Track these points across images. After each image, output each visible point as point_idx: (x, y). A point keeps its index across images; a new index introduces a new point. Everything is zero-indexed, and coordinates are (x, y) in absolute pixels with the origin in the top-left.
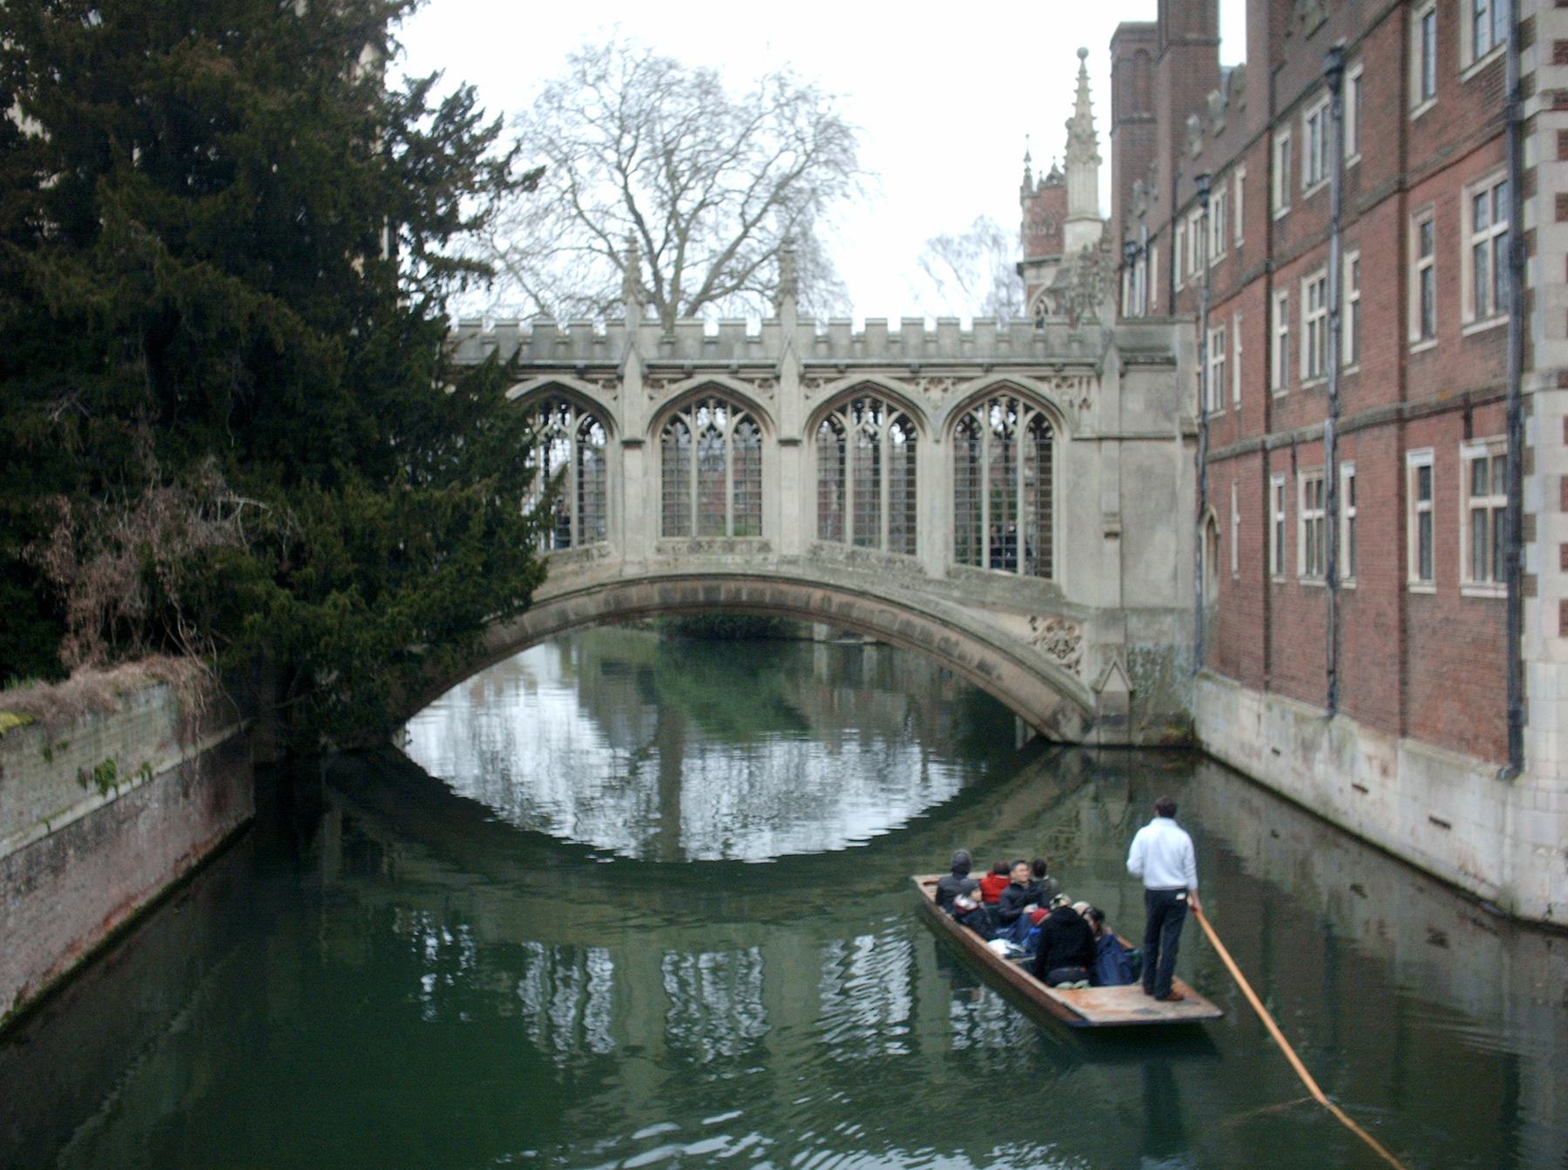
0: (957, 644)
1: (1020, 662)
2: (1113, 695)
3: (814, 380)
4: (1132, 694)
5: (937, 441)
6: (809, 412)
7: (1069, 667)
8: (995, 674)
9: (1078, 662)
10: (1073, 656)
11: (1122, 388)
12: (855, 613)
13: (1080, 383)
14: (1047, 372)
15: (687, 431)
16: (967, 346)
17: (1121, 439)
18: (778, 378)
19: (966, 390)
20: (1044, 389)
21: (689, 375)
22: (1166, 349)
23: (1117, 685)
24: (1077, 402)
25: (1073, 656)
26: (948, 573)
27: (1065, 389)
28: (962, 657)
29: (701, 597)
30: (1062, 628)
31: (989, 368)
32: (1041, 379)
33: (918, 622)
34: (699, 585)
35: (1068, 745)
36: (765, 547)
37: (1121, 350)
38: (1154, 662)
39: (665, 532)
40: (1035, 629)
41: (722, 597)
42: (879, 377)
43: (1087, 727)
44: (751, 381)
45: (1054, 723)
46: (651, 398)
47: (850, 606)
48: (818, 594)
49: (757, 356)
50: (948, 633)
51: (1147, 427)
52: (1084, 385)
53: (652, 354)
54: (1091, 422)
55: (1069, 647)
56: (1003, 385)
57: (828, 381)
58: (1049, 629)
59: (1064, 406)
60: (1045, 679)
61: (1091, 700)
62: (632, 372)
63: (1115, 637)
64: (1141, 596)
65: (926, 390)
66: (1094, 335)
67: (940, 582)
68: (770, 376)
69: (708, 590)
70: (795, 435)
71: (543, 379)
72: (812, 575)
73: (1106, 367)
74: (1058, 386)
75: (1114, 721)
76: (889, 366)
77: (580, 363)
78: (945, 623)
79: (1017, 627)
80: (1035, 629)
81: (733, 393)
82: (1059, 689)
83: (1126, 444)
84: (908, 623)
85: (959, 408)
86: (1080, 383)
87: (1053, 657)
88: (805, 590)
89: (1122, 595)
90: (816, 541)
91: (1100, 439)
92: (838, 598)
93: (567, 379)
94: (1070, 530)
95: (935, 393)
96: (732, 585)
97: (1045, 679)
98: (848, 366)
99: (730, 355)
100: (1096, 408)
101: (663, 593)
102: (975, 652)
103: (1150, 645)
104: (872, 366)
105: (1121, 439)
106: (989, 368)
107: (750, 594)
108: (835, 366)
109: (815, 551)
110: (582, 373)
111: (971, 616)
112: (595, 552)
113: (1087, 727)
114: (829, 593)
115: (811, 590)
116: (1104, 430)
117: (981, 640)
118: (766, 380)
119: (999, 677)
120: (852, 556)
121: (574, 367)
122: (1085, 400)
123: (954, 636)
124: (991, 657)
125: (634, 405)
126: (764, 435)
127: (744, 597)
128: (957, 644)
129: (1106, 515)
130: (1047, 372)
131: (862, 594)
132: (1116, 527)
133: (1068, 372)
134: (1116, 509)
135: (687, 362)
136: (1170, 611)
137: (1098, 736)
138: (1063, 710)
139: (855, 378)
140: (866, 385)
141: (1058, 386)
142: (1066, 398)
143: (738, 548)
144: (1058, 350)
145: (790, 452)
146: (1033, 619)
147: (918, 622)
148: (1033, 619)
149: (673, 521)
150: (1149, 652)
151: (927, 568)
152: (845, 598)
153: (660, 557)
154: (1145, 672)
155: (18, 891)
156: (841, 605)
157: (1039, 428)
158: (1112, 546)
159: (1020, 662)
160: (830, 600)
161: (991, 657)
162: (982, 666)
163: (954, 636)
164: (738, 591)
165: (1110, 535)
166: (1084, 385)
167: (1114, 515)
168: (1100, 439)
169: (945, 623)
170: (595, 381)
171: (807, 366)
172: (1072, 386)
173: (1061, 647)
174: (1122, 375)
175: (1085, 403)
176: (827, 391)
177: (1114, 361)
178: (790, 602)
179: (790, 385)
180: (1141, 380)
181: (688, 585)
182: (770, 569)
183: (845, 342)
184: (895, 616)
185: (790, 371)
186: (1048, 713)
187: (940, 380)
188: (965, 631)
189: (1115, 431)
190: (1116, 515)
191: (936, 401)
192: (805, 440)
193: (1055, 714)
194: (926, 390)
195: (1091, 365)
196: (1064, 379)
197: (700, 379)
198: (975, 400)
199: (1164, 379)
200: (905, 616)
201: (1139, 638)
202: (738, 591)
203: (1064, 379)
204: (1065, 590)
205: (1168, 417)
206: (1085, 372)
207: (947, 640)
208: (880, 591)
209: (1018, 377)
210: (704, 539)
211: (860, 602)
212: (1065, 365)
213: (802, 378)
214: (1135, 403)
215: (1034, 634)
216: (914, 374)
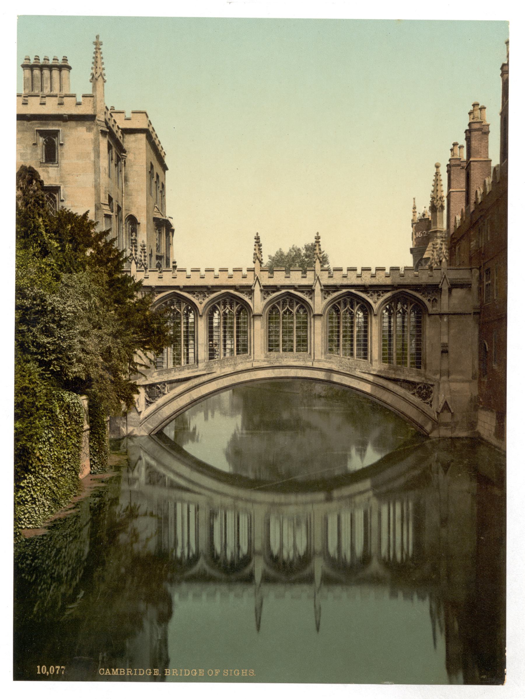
9: (431, 401)
15: (279, 311)
149: (272, 346)
170: (242, 292)
185: (318, 289)
216: (365, 288)
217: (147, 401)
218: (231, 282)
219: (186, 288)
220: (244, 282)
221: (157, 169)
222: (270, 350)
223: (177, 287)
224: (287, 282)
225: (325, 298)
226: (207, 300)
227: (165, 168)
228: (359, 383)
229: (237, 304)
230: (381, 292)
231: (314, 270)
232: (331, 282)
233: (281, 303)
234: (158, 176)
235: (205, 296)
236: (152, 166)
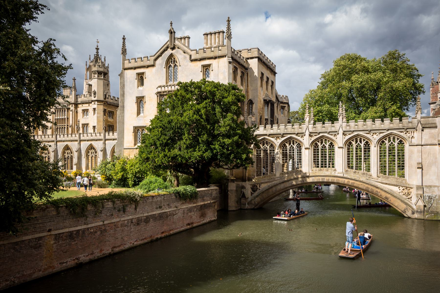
1: (395, 197)
2: (419, 206)
3: (346, 134)
4: (425, 206)
7: (409, 199)
8: (389, 200)
9: (411, 198)
10: (410, 196)
12: (355, 185)
16: (382, 125)
17: (422, 145)
19: (382, 135)
20: (402, 134)
21: (319, 134)
22: (435, 123)
23: (421, 204)
24: (411, 137)
25: (410, 196)
28: (381, 195)
29: (321, 181)
31: (388, 130)
32: (401, 132)
34: (320, 178)
35: (409, 218)
36: (335, 170)
38: (432, 198)
41: (325, 181)
42: (361, 133)
43: (413, 213)
44: (331, 135)
45: (405, 212)
47: (354, 183)
49: (333, 129)
51: (429, 143)
52: (412, 133)
53: (311, 130)
54: (414, 141)
55: (409, 194)
56: (391, 134)
57: (350, 134)
58: (403, 190)
59: (407, 138)
61: (415, 207)
62: (307, 133)
64: (428, 184)
65: (372, 135)
66: (415, 121)
68: (336, 133)
69: (322, 179)
71: (289, 136)
72: (345, 176)
74: (406, 133)
77: (296, 133)
78: (377, 188)
81: (328, 138)
82: (406, 204)
85: (380, 139)
87: (404, 196)
88: (343, 179)
92: (351, 181)
93: (294, 136)
94: (409, 167)
95: (375, 136)
96: (327, 178)
98: (354, 131)
99: (328, 130)
100: (416, 138)
101: (313, 179)
102: (384, 195)
103: (429, 195)
105: (422, 145)
106: (388, 130)
107: (331, 180)
108: (350, 131)
110: (297, 134)
113: (413, 213)
117: (385, 191)
118: (335, 135)
120: (355, 172)
124: (389, 196)
127: (330, 181)
129: (418, 163)
136: (436, 186)
138: (407, 209)
139: (355, 133)
140: (358, 135)
141: (406, 133)
142: (408, 136)
143: (329, 170)
144: (406, 125)
145: (341, 149)
146: (399, 187)
148: (399, 187)
150: (430, 196)
151: (373, 175)
154: (429, 201)
155: (135, 225)
156: (352, 183)
157: (401, 142)
159: (395, 197)
161: (389, 196)
163: (379, 190)
164: (329, 179)
165: (418, 168)
166: (412, 133)
167: (420, 163)
168: (416, 145)
170: (299, 136)
171: (344, 131)
173: (407, 194)
178: (340, 182)
179: (340, 135)
181: (318, 178)
182: (336, 174)
186: (403, 209)
187: (376, 133)
188: (382, 189)
189: (420, 143)
191: (374, 138)
192: (344, 147)
193: (405, 210)
194: (372, 135)
195: (414, 128)
197: (321, 135)
198: (384, 137)
199: (433, 131)
200: (367, 186)
201: (427, 193)
202: (329, 179)
203: (407, 132)
204: (407, 181)
205: (435, 139)
206: (412, 130)
207: (377, 191)
208: (361, 179)
210: (322, 168)
212: (407, 129)
215: (399, 191)
217: (251, 193)
218: (293, 131)
219: (270, 135)
220: (300, 131)
221: (267, 73)
223: (266, 135)
224: (323, 130)
227: (274, 73)
232: (348, 129)
234: (268, 78)
236: (262, 74)
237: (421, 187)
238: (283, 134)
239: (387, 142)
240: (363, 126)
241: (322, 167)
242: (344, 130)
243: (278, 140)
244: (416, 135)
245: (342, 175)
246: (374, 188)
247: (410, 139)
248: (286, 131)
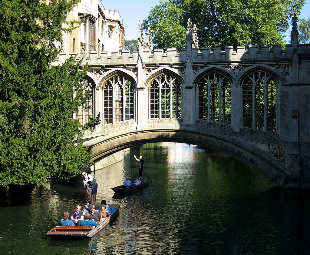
0: (243, 153)
1: (263, 159)
5: (237, 87)
6: (195, 78)
7: (281, 162)
8: (255, 163)
9: (284, 160)
11: (299, 68)
13: (285, 67)
14: (274, 63)
15: (158, 85)
17: (298, 85)
18: (185, 67)
20: (273, 69)
24: (284, 73)
26: (241, 130)
27: (280, 69)
30: (279, 148)
31: (254, 62)
32: (272, 65)
33: (230, 145)
37: (299, 55)
39: (152, 116)
40: (270, 149)
42: (217, 66)
43: (286, 182)
46: (147, 75)
47: (208, 140)
48: (197, 136)
50: (239, 149)
52: (287, 67)
53: (146, 61)
54: (290, 79)
56: (259, 68)
57: (202, 68)
60: (273, 165)
63: (295, 152)
67: (237, 133)
70: (191, 85)
72: (195, 129)
73: (293, 60)
74: (277, 68)
75: (294, 180)
76: (221, 62)
77: (125, 64)
79: (263, 147)
80: (270, 149)
82: (278, 169)
83: (300, 87)
84: (227, 146)
85: (244, 76)
86: (285, 67)
88: (193, 135)
89: (298, 138)
90: (198, 119)
91: (292, 85)
92: (204, 138)
93: (121, 69)
97: (273, 165)
98: (208, 63)
100: (291, 75)
104: (215, 63)
105: (298, 85)
108: (203, 63)
109: (197, 122)
111: (249, 144)
112: (130, 123)
114: (201, 136)
115: (195, 135)
116: (293, 82)
119: (257, 164)
121: (123, 65)
122: (287, 72)
123: (242, 151)
124: (254, 157)
125: (142, 78)
126: (181, 86)
128: (243, 153)
130: (274, 63)
131: (212, 136)
132: (296, 114)
133: (281, 63)
134: (297, 109)
135: (157, 63)
137: (290, 185)
139: (211, 66)
141: (277, 68)
144: (277, 56)
145: (189, 91)
146: (269, 146)
147: (230, 145)
148: (269, 146)
149: (154, 113)
152: (206, 138)
153: (150, 125)
158: (295, 121)
159: (263, 159)
160: (201, 138)
161: (254, 157)
162: (252, 161)
165: (293, 117)
167: (295, 110)
168: (292, 85)
169: (239, 146)
170: (130, 70)
171: (194, 63)
172: (282, 68)
174: (299, 64)
175: (287, 73)
176: (202, 71)
177: (296, 58)
180: (304, 65)
183: (207, 55)
184: (222, 143)
188: (244, 149)
189: (296, 82)
190: (298, 111)
195: (289, 60)
196: (280, 65)
200: (226, 144)
203: (280, 65)
206: (286, 63)
207: (239, 152)
209: (263, 65)
211: (211, 139)
213: (193, 67)
214: (303, 73)
218: (120, 62)
220: (131, 62)
222: (152, 116)
224: (165, 61)
225: (195, 73)
226: (102, 76)
228: (175, 144)
229: (222, 77)
230: (241, 67)
231: (186, 50)
233: (160, 78)
235: (101, 74)
237: (297, 144)
238: (106, 66)
239: (253, 79)
240: (221, 57)
241: (163, 116)
242: (194, 60)
243: (98, 75)
244: (292, 71)
245: (190, 129)
246: (235, 147)
247: (284, 75)
248: (109, 62)
